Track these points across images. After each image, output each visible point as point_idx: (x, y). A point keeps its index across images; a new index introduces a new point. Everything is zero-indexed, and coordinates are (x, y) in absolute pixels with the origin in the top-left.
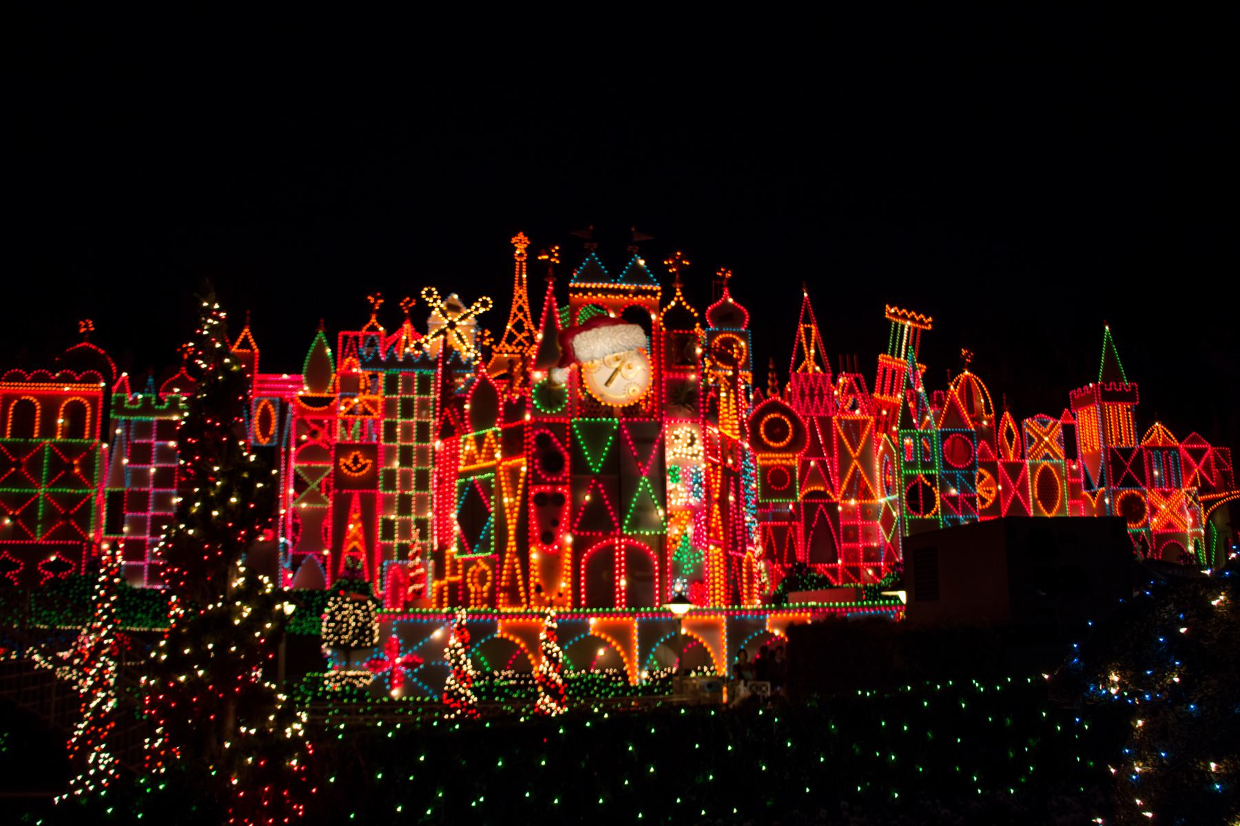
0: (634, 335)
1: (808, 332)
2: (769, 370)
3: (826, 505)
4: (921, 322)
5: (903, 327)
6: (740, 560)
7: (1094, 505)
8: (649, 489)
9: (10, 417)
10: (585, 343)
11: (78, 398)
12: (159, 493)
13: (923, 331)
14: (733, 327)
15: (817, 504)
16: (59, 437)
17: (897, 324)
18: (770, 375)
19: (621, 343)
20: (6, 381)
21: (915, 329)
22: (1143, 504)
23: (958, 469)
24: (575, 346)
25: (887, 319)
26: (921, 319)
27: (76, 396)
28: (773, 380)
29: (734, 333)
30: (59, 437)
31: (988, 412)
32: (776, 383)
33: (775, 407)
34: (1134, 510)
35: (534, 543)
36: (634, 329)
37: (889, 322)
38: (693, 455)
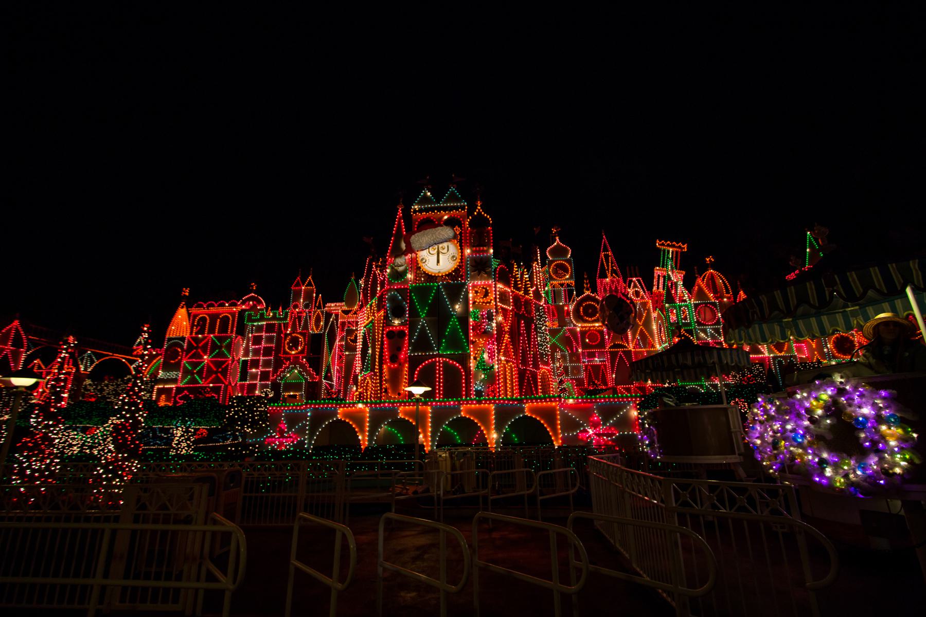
0: (448, 232)
1: (607, 256)
2: (584, 279)
3: (624, 352)
4: (680, 247)
5: (668, 252)
6: (534, 376)
7: (814, 346)
8: (457, 325)
9: (207, 329)
10: (417, 239)
11: (226, 314)
12: (265, 359)
13: (682, 253)
14: (563, 257)
15: (619, 351)
16: (216, 334)
17: (664, 251)
18: (585, 281)
19: (438, 236)
20: (195, 308)
21: (677, 252)
22: (852, 342)
23: (708, 325)
24: (411, 241)
25: (658, 248)
26: (680, 246)
27: (225, 313)
28: (587, 284)
29: (563, 261)
30: (216, 334)
31: (728, 292)
32: (588, 286)
33: (588, 298)
34: (846, 347)
35: (386, 363)
36: (447, 229)
37: (659, 250)
38: (486, 303)
